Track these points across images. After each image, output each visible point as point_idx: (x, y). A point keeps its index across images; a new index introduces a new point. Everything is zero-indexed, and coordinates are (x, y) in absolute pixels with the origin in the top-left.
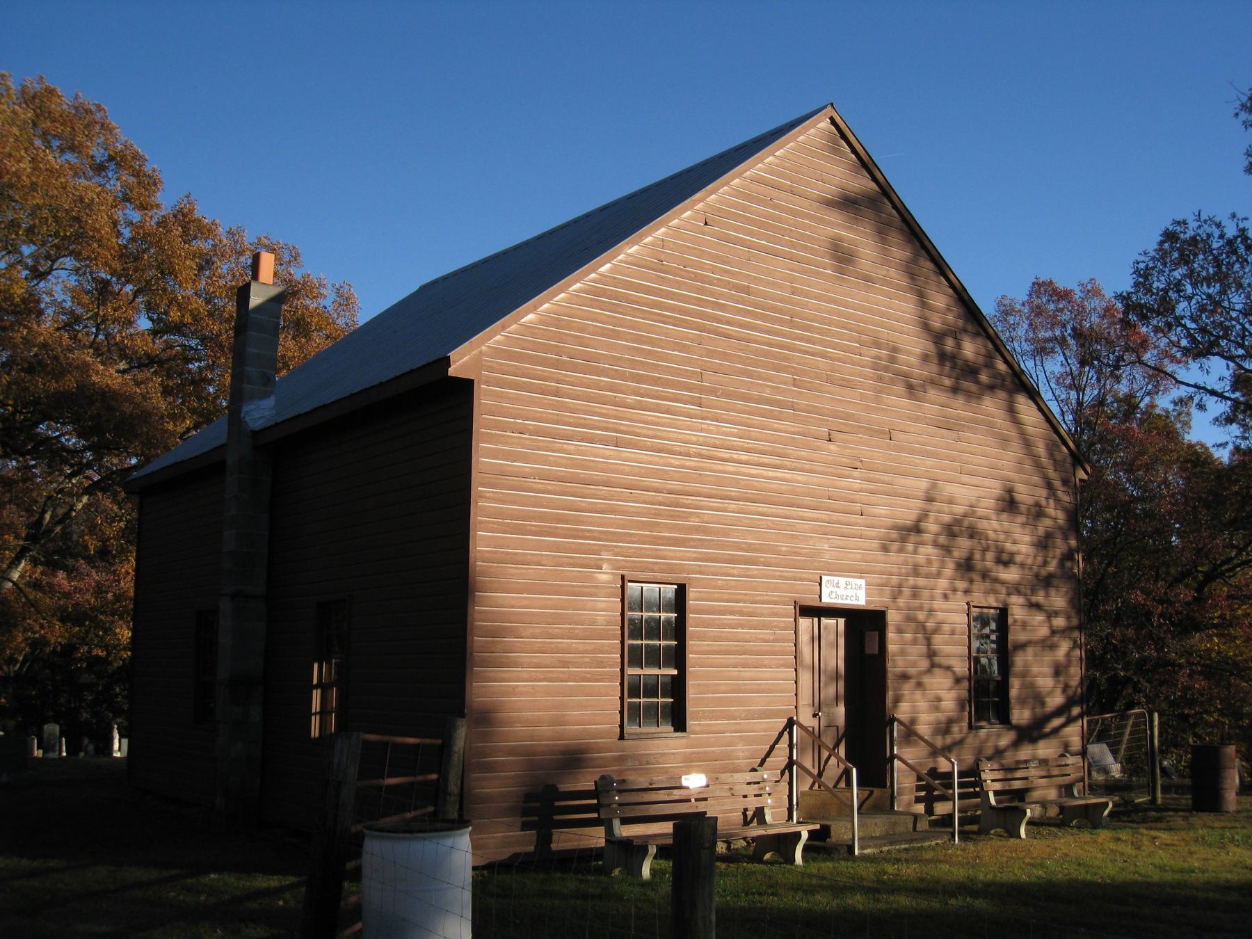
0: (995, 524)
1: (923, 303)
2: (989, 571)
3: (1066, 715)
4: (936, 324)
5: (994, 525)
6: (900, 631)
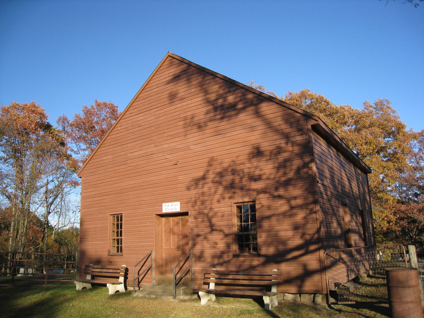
0: (248, 165)
1: (206, 92)
2: (245, 186)
3: (305, 249)
4: (213, 97)
6: (195, 218)
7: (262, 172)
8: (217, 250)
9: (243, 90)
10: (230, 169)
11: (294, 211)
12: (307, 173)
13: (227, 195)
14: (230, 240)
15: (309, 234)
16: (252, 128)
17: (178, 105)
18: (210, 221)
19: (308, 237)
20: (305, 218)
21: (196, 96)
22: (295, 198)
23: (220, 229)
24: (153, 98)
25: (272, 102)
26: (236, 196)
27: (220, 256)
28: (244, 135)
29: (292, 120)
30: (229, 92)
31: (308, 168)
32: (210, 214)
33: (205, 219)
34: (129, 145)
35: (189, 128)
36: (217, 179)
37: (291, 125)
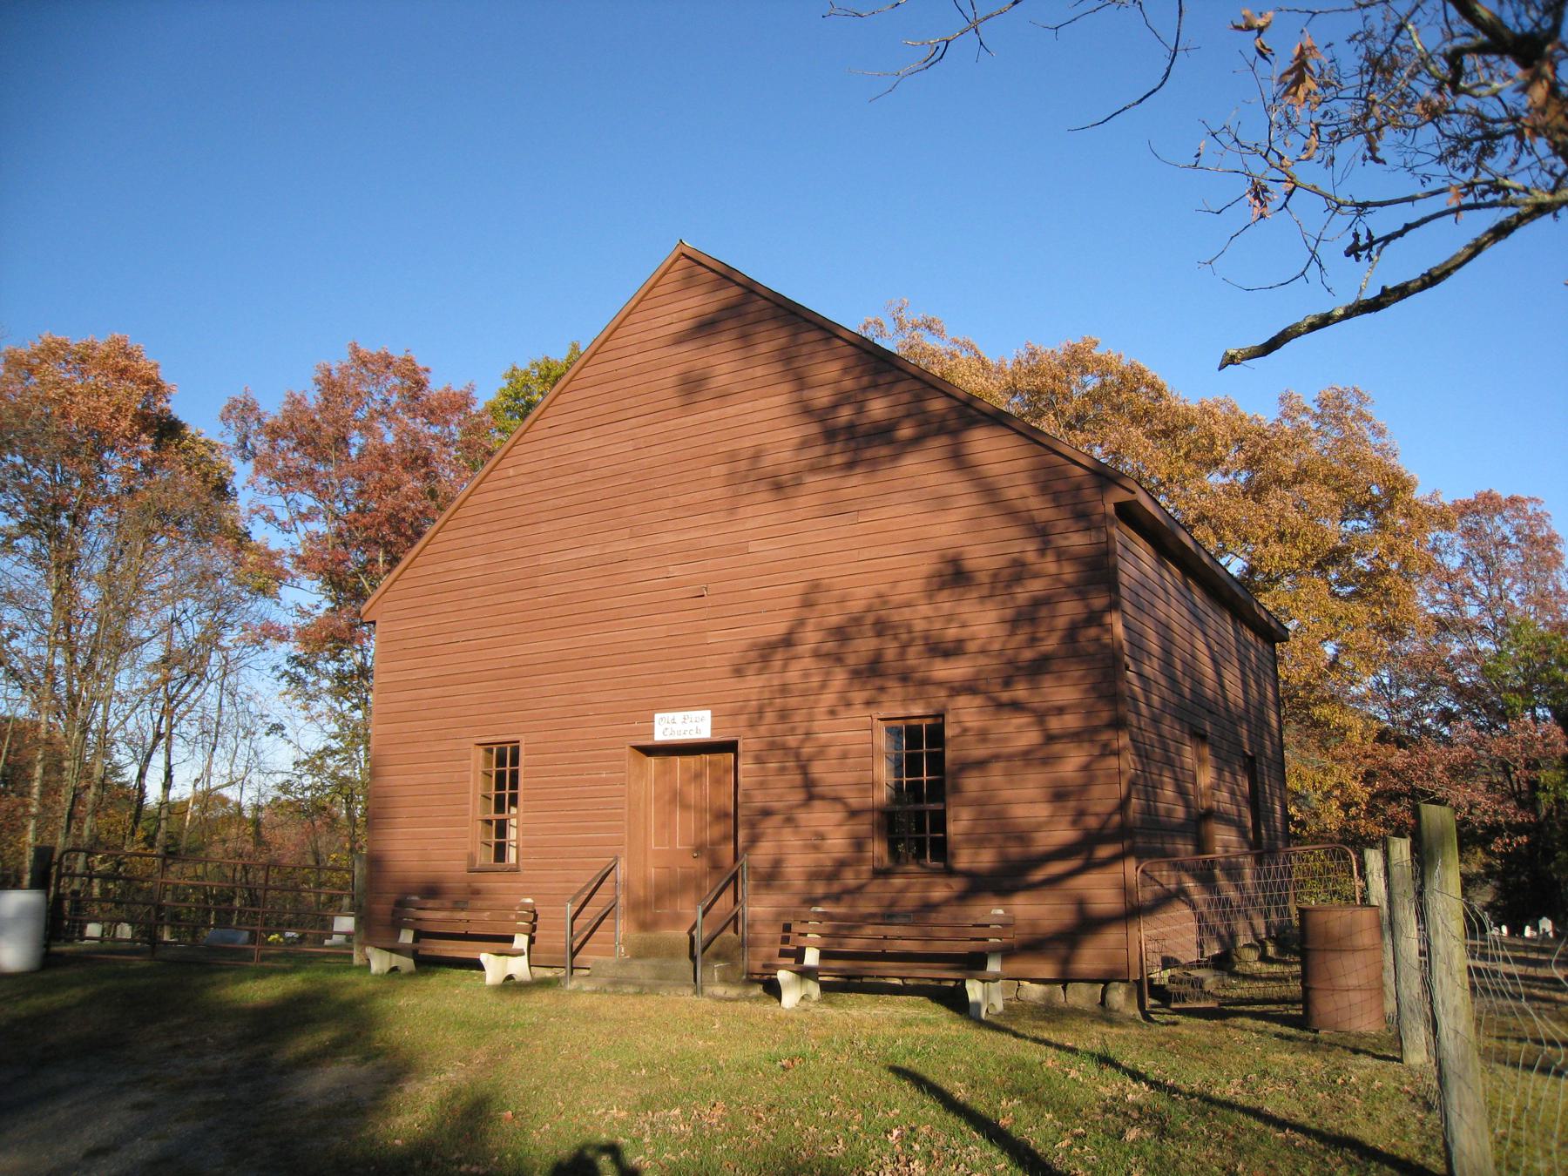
0: (925, 610)
1: (800, 382)
2: (913, 670)
3: (1083, 856)
4: (822, 397)
5: (922, 616)
6: (759, 760)
7: (965, 633)
8: (821, 855)
9: (918, 386)
10: (870, 618)
11: (1057, 748)
12: (1097, 639)
13: (859, 696)
14: (863, 826)
15: (1097, 815)
16: (941, 503)
17: (708, 415)
18: (804, 769)
19: (1092, 822)
20: (1086, 768)
21: (771, 390)
22: (1060, 710)
23: (833, 794)
24: (627, 383)
25: (1004, 428)
26: (884, 698)
27: (833, 875)
28: (917, 520)
29: (1060, 486)
30: (875, 386)
31: (1101, 625)
32: (807, 750)
33: (787, 764)
34: (544, 527)
35: (745, 488)
36: (830, 646)
37: (1056, 498)
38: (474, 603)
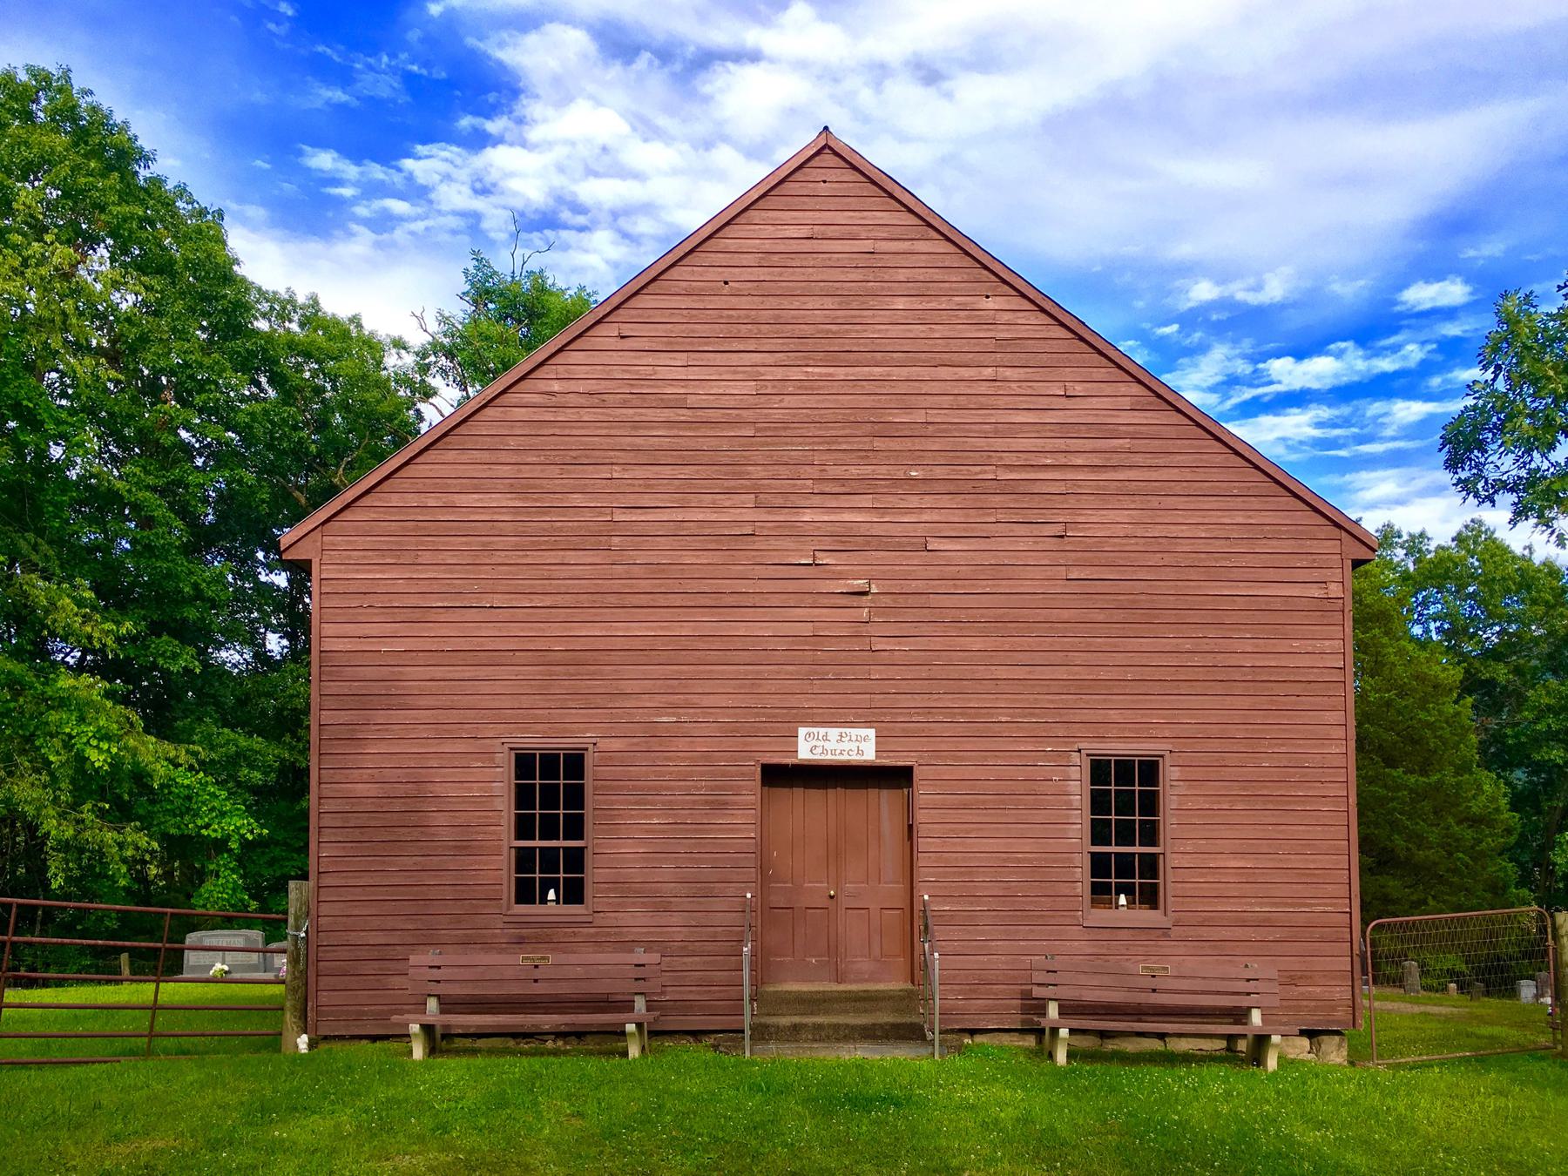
28: (1137, 544)
38: (499, 558)
